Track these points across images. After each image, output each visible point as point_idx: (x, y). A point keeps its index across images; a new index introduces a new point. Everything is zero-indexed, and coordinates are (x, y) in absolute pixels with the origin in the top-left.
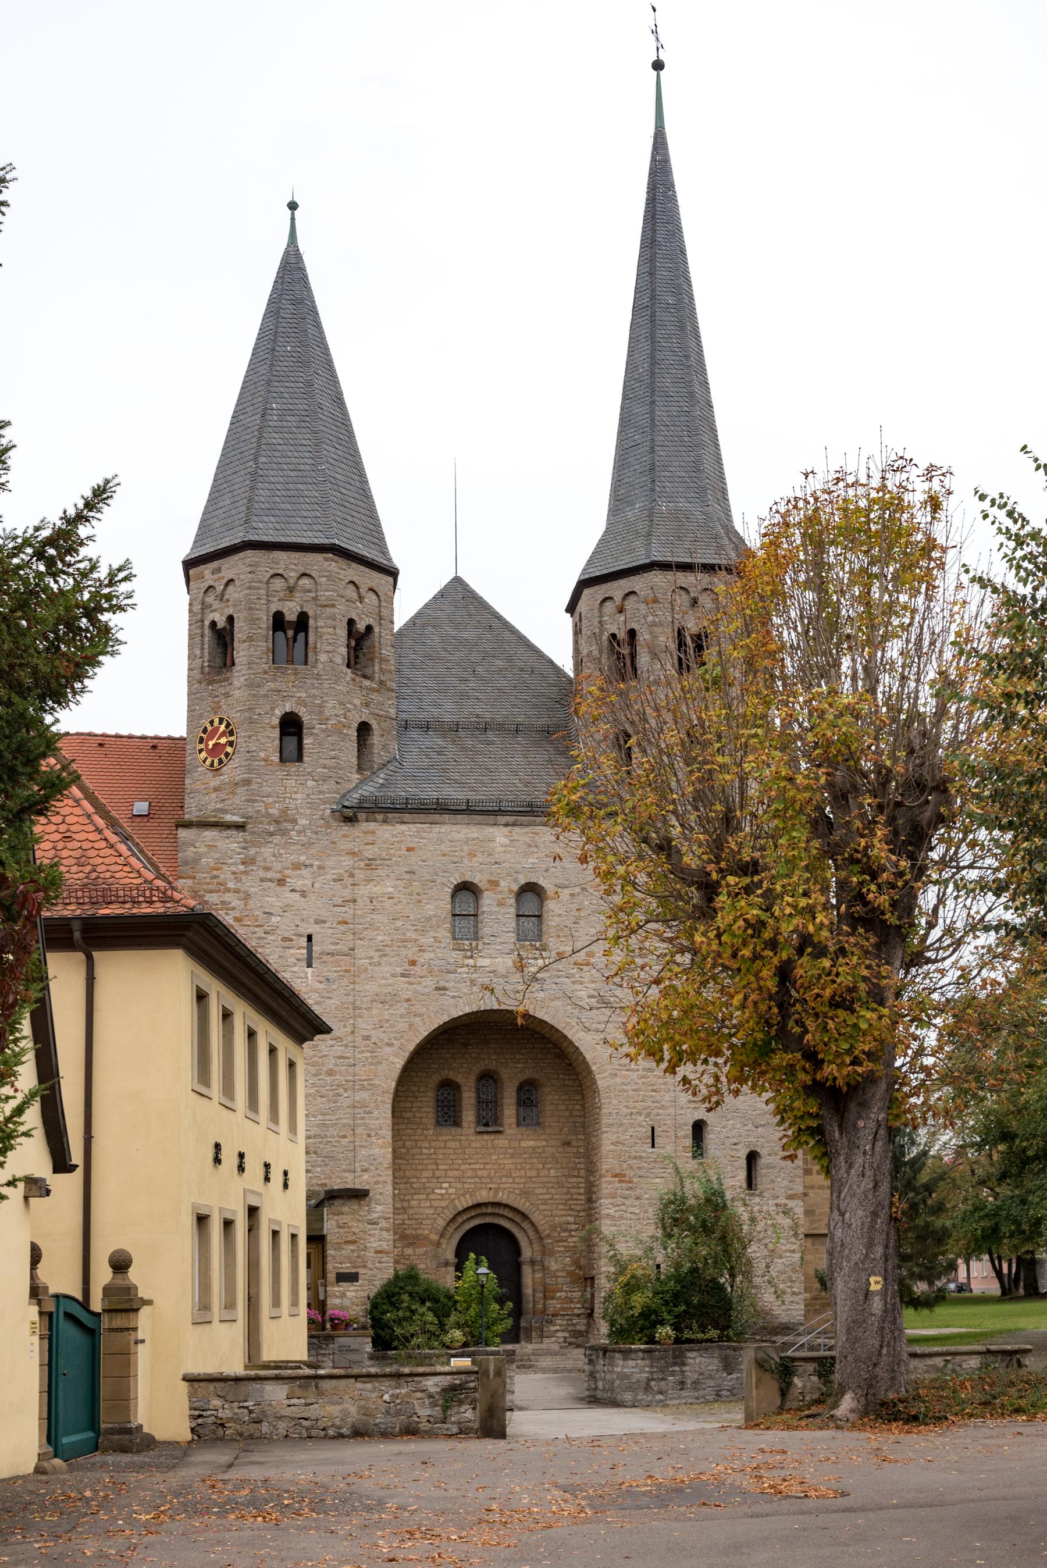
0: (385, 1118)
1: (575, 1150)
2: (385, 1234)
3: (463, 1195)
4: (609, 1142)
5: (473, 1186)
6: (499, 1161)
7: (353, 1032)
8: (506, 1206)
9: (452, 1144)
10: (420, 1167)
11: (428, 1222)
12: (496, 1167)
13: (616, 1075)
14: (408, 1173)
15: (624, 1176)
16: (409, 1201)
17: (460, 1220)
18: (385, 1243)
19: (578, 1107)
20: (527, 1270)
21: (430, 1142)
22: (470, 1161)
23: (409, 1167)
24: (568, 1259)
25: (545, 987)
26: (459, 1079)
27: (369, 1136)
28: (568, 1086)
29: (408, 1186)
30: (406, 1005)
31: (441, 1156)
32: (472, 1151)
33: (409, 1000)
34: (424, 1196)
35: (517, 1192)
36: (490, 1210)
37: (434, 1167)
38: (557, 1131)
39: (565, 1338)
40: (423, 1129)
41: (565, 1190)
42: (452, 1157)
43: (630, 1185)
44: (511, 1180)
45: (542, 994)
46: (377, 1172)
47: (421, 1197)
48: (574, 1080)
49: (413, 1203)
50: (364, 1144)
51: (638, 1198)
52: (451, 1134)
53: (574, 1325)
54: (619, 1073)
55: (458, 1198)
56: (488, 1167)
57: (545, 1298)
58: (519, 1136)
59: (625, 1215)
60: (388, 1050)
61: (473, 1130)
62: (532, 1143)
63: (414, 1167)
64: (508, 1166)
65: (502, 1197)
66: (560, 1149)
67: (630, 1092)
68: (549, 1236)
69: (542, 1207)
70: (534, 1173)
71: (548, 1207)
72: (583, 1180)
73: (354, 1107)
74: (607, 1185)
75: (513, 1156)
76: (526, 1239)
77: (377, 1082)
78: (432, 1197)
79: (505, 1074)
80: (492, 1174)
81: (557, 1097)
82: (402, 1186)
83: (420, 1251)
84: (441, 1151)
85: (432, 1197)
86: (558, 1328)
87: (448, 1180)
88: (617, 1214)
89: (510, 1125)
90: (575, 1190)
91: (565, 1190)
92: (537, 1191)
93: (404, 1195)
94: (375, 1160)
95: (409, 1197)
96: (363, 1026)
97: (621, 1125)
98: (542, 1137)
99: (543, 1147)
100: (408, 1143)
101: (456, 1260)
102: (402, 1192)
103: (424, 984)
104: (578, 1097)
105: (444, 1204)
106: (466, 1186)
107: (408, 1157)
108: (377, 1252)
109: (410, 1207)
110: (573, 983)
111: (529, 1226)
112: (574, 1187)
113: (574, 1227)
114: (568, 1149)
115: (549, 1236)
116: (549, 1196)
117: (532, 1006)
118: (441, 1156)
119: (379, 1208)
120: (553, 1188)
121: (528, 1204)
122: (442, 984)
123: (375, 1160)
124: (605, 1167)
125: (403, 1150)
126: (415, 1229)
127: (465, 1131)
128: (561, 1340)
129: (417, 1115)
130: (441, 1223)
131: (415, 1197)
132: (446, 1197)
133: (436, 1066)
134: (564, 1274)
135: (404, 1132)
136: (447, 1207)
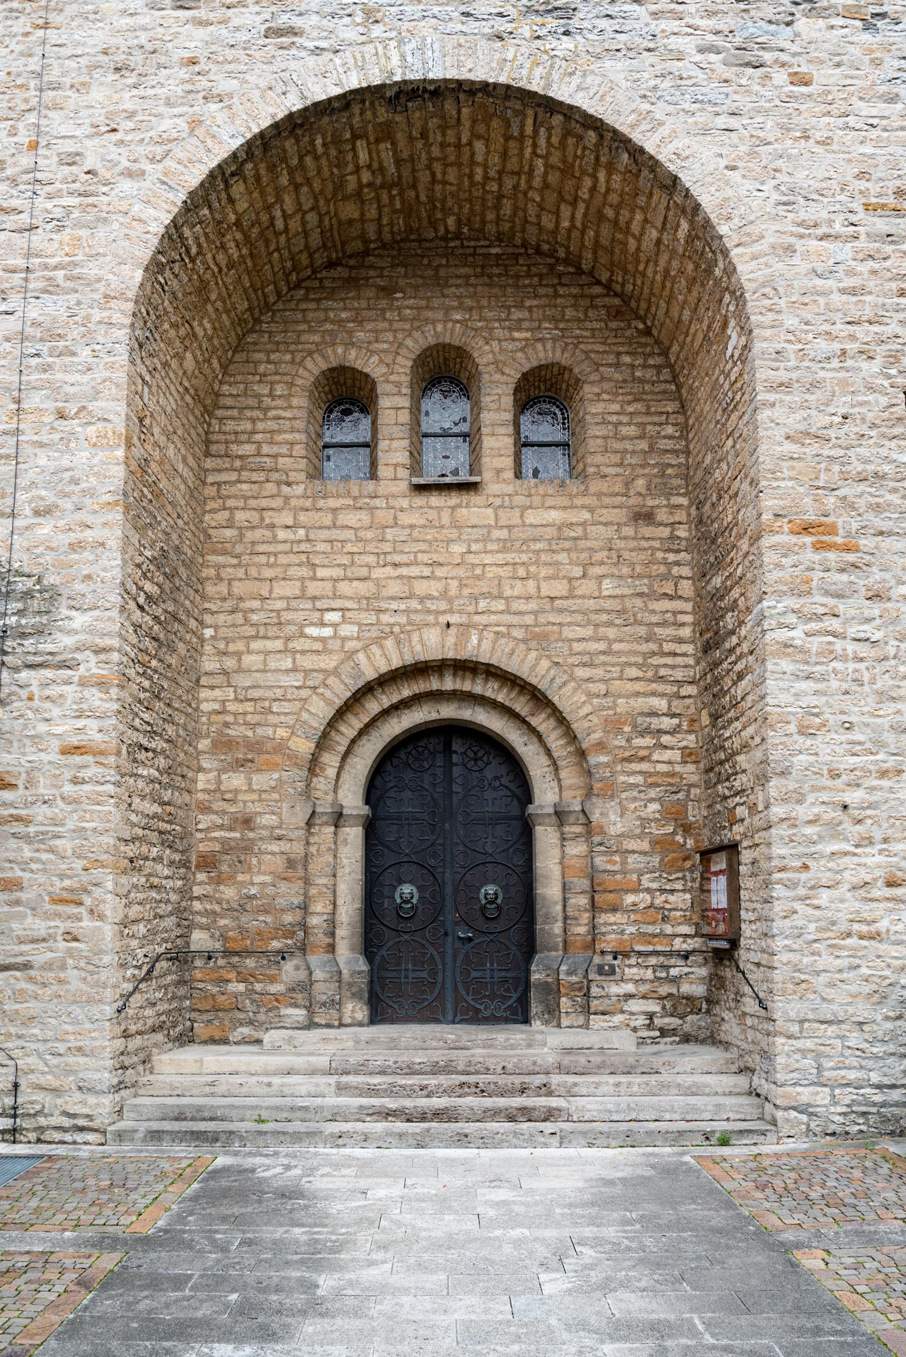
0: (111, 366)
1: (665, 532)
2: (95, 698)
3: (378, 641)
4: (779, 434)
5: (403, 619)
6: (471, 559)
7: (34, 146)
8: (491, 672)
9: (350, 518)
10: (268, 573)
11: (287, 707)
12: (461, 572)
13: (790, 250)
14: (238, 588)
15: (832, 530)
16: (238, 655)
17: (373, 707)
18: (93, 724)
19: (670, 430)
21: (296, 511)
22: (397, 558)
23: (240, 573)
24: (655, 806)
25: (575, 23)
26: (373, 367)
27: (62, 416)
28: (642, 381)
29: (239, 618)
30: (183, 73)
31: (321, 547)
32: (403, 534)
33: (193, 62)
34: (278, 644)
35: (518, 633)
36: (449, 683)
37: (304, 572)
38: (618, 487)
39: (651, 1016)
40: (279, 483)
41: (642, 631)
42: (349, 547)
43: (851, 557)
44: (500, 605)
45: (567, 43)
46: (78, 516)
47: (270, 645)
48: (658, 368)
49: (248, 660)
50: (45, 438)
51: (875, 597)
52: (348, 494)
53: (675, 980)
54: (799, 244)
55: (365, 648)
56: (440, 572)
57: (594, 907)
58: (520, 500)
59: (839, 645)
60: (126, 186)
61: (403, 486)
62: (555, 516)
63: (253, 572)
64: (491, 572)
65: (479, 647)
66: (629, 531)
67: (836, 297)
68: (601, 746)
69: (581, 673)
70: (559, 588)
71: (599, 672)
72: (688, 607)
73: (23, 337)
74: (779, 561)
75: (505, 546)
76: (544, 760)
77: (91, 270)
78: (297, 645)
79: (484, 354)
80: (453, 592)
81: (616, 407)
82: (221, 618)
83: (261, 780)
84: (324, 534)
85: (297, 645)
87: (338, 604)
88: (815, 644)
89: (499, 471)
90: (670, 631)
91: (642, 631)
92: (568, 633)
93: (228, 641)
94: (75, 481)
95: (240, 646)
96: (63, 130)
97: (814, 385)
98: (578, 502)
99: (584, 524)
100: (240, 516)
101: (366, 810)
102: (222, 632)
103: (236, 22)
104: (671, 407)
105: (329, 662)
106: (385, 618)
107: (239, 549)
108: (68, 751)
109: (240, 670)
110: (655, 15)
111: (552, 723)
112: (664, 624)
113: (667, 723)
114: (647, 531)
115: (601, 746)
116: (602, 646)
117: (539, 72)
118: (321, 547)
119: (80, 620)
120: (610, 624)
121: (545, 664)
122: (284, 20)
123: (75, 481)
124: (769, 503)
125: (228, 533)
126: (253, 726)
127: (384, 487)
128: (641, 1021)
129: (265, 449)
130: (320, 710)
131: (255, 645)
132: (335, 645)
133: (316, 338)
134: (645, 846)
135: (234, 490)
136: (335, 672)
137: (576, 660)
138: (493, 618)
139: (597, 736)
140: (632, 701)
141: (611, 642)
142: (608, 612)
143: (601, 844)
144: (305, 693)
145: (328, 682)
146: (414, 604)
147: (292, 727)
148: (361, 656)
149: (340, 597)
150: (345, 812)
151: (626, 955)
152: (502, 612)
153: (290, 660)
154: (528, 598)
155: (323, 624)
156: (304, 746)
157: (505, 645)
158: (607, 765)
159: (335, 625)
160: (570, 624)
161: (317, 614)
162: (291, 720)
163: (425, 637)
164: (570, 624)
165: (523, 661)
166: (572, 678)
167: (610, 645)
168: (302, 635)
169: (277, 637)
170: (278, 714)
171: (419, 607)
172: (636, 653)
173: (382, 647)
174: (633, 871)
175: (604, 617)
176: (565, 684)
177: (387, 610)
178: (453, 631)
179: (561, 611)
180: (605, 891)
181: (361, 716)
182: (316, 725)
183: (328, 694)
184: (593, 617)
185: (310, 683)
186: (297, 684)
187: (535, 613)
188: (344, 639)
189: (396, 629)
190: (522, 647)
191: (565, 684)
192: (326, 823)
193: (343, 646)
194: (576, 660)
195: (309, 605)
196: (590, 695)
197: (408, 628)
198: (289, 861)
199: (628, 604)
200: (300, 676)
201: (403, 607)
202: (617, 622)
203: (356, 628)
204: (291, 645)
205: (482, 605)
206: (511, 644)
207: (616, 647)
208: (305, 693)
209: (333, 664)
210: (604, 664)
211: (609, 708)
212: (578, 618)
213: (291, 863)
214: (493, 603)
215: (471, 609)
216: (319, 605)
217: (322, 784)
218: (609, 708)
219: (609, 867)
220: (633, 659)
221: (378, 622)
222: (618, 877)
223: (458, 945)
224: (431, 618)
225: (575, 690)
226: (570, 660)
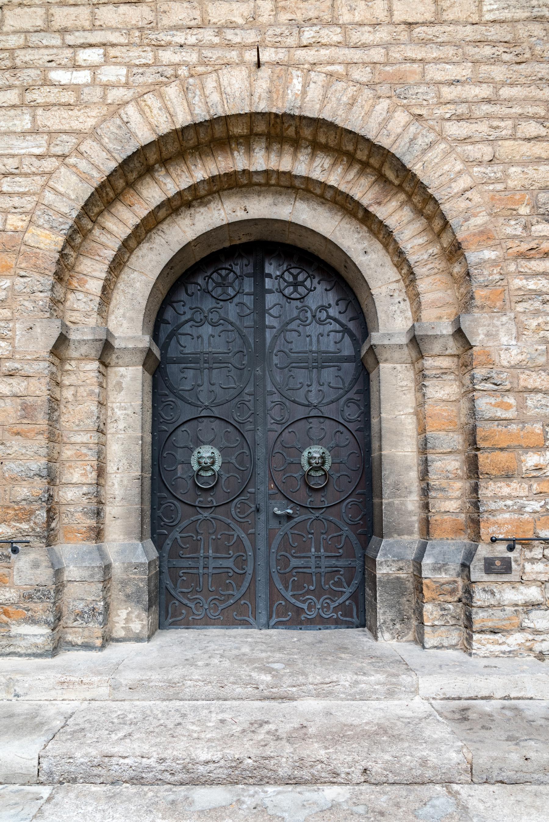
3: (156, 89)
5: (193, 57)
11: (22, 184)
20: (394, 382)
35: (361, 74)
36: (260, 160)
44: (334, 35)
55: (138, 99)
57: (473, 468)
65: (305, 96)
68: (485, 236)
69: (454, 129)
76: (391, 273)
78: (39, 96)
80: (265, 18)
85: (39, 96)
86: (533, 593)
92: (435, 73)
101: (145, 341)
105: (85, 120)
106: (167, 56)
115: (485, 236)
120: (495, 60)
121: (401, 117)
130: (72, 190)
136: (94, 134)
137: (447, 111)
138: (324, 53)
139: (480, 220)
140: (530, 170)
141: (497, 85)
142: (493, 44)
143: (486, 380)
144: (49, 164)
145: (83, 148)
146: (208, 35)
147: (31, 213)
148: (131, 110)
149: (101, 28)
150: (117, 344)
151: (527, 543)
152: (337, 45)
153: (27, 118)
154: (376, 25)
155: (76, 67)
156: (48, 241)
157: (342, 92)
158: (495, 263)
159: (94, 68)
160: (437, 61)
161: (68, 52)
162: (28, 203)
163: (225, 82)
164: (437, 61)
165: (368, 114)
166: (442, 136)
167: (496, 90)
168: (46, 82)
169: (10, 87)
170: (10, 194)
171: (216, 40)
172: (535, 101)
173: (161, 96)
174: (535, 419)
175: (487, 51)
176: (431, 145)
177: (169, 44)
178: (265, 72)
179: (424, 42)
180: (493, 449)
181: (136, 208)
182: (66, 210)
183: (83, 165)
184: (471, 50)
185: (58, 150)
186: (37, 151)
187: (387, 46)
188: (106, 86)
189: (183, 71)
190: (367, 93)
191: (431, 145)
192: (86, 358)
193: (104, 97)
194: (447, 111)
195: (56, 40)
196: (469, 162)
197: (201, 69)
198: (25, 407)
199: (522, 31)
200: (43, 140)
201: (192, 40)
202: (506, 57)
203: (123, 71)
204: (29, 97)
205: (308, 35)
206: (351, 90)
207: (506, 92)
208: (49, 164)
209: (91, 122)
210: (488, 117)
211: (498, 180)
212: (450, 51)
213: (27, 411)
214: (324, 32)
215: (291, 41)
216: (70, 39)
217: (81, 303)
218: (498, 180)
219: (500, 413)
220: (531, 110)
221: (157, 62)
222: (514, 427)
223: (274, 524)
224: (233, 55)
225: (446, 154)
226: (441, 111)
